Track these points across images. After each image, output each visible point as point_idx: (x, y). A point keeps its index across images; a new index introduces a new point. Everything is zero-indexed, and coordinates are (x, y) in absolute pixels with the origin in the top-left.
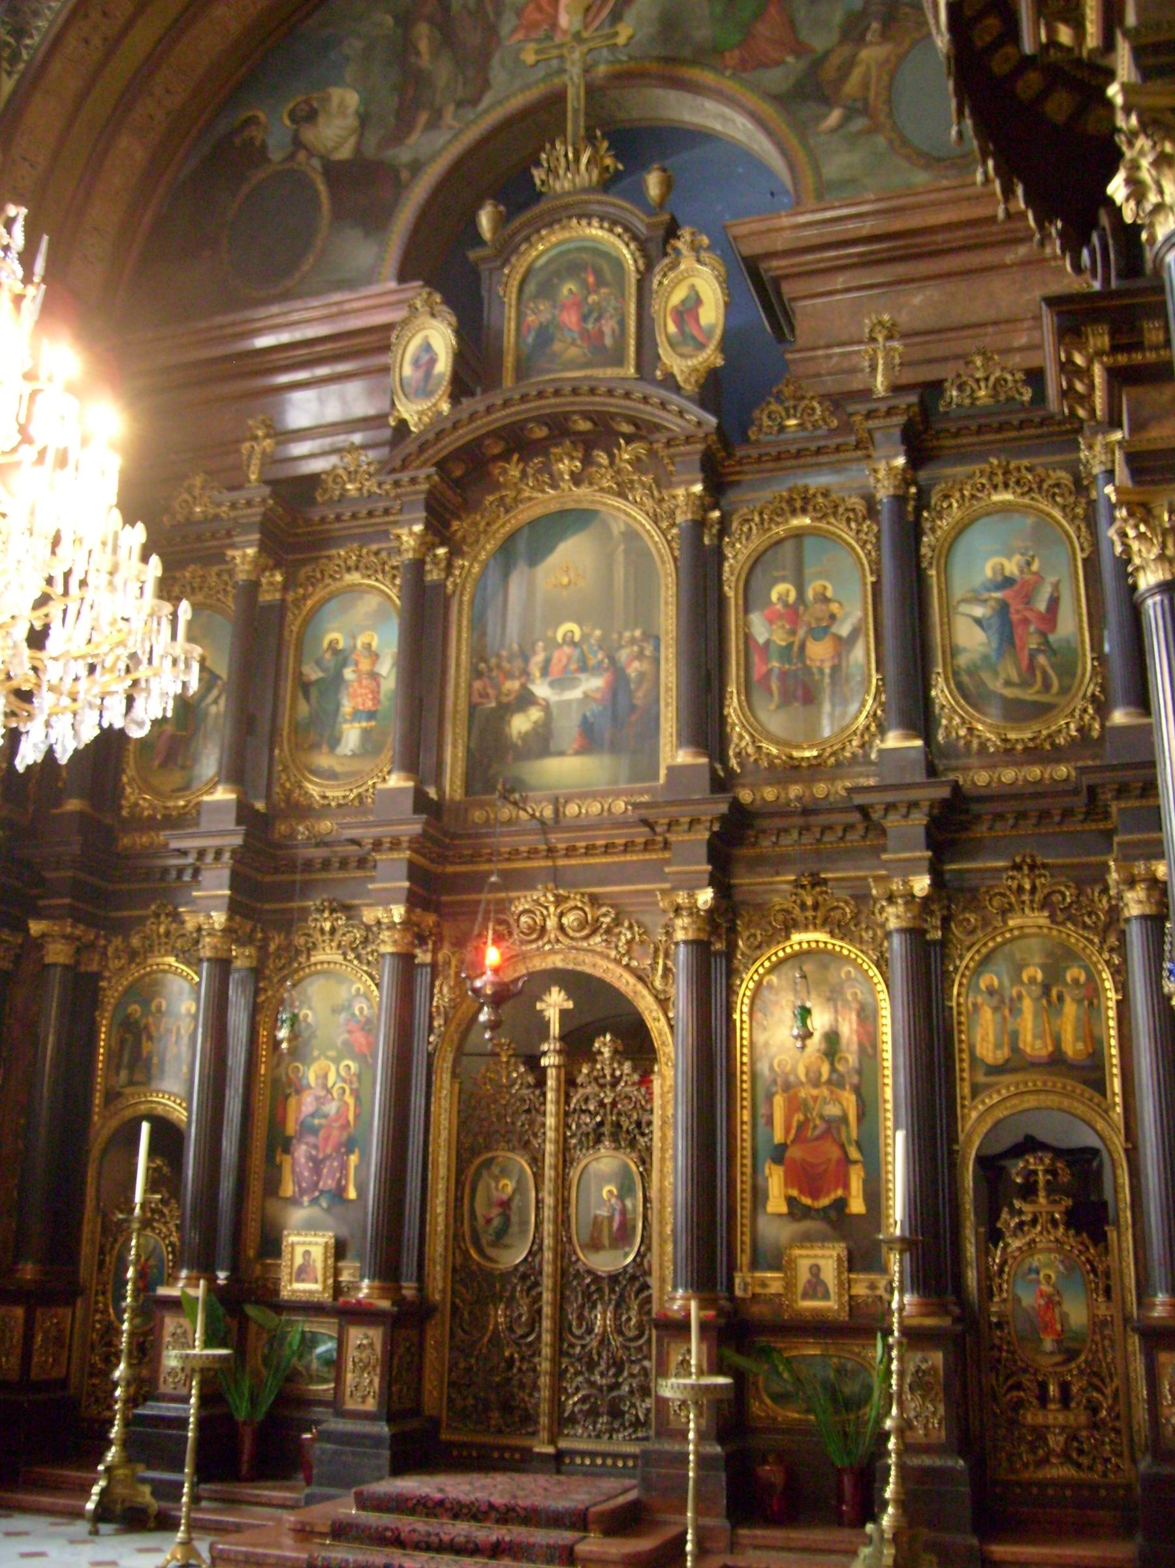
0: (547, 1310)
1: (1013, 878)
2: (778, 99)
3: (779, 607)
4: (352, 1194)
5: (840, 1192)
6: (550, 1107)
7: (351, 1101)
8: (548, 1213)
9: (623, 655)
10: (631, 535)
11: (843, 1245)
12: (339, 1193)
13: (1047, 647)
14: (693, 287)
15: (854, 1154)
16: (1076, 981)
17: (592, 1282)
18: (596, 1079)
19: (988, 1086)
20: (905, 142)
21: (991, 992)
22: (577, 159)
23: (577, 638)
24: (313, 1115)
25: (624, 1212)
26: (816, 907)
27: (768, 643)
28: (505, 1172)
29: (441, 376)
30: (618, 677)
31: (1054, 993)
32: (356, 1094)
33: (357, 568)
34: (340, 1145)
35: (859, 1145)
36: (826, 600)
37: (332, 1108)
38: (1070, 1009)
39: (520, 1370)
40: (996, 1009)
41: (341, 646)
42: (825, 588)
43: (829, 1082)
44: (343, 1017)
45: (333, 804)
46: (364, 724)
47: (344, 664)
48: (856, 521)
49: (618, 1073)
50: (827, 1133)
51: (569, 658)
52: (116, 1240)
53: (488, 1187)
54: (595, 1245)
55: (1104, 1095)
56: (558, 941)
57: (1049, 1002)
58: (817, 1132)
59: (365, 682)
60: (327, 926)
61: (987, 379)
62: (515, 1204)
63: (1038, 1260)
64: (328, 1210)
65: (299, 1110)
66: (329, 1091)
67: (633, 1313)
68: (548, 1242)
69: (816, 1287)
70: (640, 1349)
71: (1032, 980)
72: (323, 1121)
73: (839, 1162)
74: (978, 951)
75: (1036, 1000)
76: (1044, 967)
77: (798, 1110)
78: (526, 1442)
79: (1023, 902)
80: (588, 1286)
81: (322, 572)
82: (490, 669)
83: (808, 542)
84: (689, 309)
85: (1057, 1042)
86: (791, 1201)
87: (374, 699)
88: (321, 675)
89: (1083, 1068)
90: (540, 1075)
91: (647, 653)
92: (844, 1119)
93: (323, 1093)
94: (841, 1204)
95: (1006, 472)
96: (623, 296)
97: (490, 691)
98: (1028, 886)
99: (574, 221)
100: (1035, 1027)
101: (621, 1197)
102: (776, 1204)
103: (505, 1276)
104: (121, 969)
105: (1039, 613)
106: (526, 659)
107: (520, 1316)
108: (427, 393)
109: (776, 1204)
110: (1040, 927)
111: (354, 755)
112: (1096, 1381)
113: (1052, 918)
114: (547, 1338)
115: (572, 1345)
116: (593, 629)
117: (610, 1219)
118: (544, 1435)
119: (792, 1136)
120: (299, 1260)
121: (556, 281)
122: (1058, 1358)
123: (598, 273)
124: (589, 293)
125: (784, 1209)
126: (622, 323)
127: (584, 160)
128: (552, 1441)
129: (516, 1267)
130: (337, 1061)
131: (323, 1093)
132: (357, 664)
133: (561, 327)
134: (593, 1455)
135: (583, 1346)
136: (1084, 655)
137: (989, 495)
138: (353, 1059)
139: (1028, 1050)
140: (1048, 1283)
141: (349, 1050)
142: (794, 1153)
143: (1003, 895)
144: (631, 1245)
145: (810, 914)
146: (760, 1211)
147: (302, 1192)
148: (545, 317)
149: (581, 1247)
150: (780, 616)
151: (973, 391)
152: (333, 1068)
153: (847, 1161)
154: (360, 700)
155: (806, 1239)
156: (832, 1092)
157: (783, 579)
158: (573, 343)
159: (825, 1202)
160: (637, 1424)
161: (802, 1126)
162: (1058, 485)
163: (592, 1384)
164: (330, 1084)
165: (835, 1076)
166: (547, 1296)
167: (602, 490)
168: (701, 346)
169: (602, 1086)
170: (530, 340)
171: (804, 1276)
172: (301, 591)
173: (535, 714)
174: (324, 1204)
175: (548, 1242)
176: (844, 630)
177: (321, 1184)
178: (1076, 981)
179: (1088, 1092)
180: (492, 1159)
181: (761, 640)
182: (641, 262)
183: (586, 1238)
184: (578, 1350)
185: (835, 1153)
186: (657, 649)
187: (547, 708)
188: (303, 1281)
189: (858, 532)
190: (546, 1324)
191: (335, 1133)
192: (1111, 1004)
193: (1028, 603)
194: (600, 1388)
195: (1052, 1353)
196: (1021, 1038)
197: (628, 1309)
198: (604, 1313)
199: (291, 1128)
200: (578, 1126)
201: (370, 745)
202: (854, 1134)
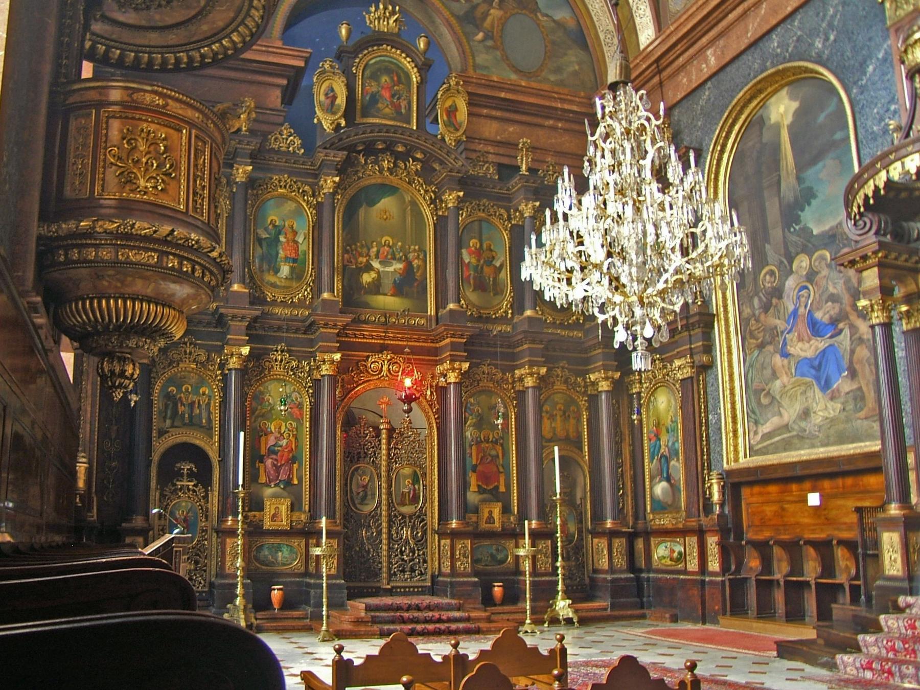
0: (384, 530)
3: (473, 249)
4: (296, 482)
6: (384, 447)
7: (293, 440)
8: (384, 491)
9: (411, 256)
10: (414, 204)
12: (288, 483)
14: (454, 101)
15: (501, 470)
16: (574, 411)
17: (402, 519)
19: (546, 447)
21: (547, 412)
23: (391, 244)
24: (274, 446)
25: (414, 490)
26: (488, 373)
27: (469, 262)
28: (364, 473)
29: (339, 106)
30: (409, 264)
31: (567, 414)
35: (503, 468)
36: (491, 250)
39: (373, 556)
40: (548, 419)
41: (277, 224)
43: (492, 441)
45: (279, 300)
47: (279, 233)
50: (492, 460)
51: (388, 253)
52: (168, 504)
54: (403, 504)
56: (387, 376)
58: (488, 460)
60: (279, 358)
61: (553, 175)
62: (369, 487)
64: (284, 489)
65: (266, 443)
66: (282, 435)
67: (419, 531)
68: (384, 502)
69: (490, 519)
70: (422, 544)
72: (279, 448)
75: (561, 416)
78: (378, 585)
80: (400, 520)
81: (267, 184)
82: (352, 251)
83: (484, 225)
84: (452, 112)
85: (567, 431)
86: (479, 486)
87: (296, 253)
91: (421, 257)
92: (498, 456)
94: (497, 488)
96: (410, 91)
97: (353, 261)
101: (413, 484)
102: (473, 488)
103: (366, 516)
104: (164, 368)
106: (369, 250)
108: (334, 113)
109: (473, 488)
113: (567, 387)
114: (385, 541)
115: (393, 545)
116: (398, 242)
117: (409, 493)
118: (385, 581)
120: (273, 512)
121: (379, 73)
123: (399, 77)
124: (394, 86)
125: (477, 490)
126: (410, 103)
128: (388, 584)
131: (279, 435)
132: (286, 234)
133: (381, 96)
134: (405, 587)
141: (291, 416)
142: (479, 468)
144: (418, 503)
145: (486, 376)
148: (374, 89)
150: (474, 253)
152: (284, 424)
155: (484, 501)
157: (475, 238)
158: (387, 106)
159: (491, 487)
160: (421, 574)
163: (403, 560)
166: (384, 525)
167: (401, 179)
168: (457, 130)
170: (368, 98)
171: (486, 515)
172: (255, 192)
173: (373, 275)
174: (282, 486)
175: (384, 502)
176: (498, 264)
178: (574, 411)
179: (577, 451)
180: (359, 467)
181: (467, 261)
182: (419, 78)
183: (399, 501)
184: (396, 546)
186: (425, 256)
187: (378, 272)
188: (275, 521)
190: (384, 536)
191: (286, 454)
194: (406, 561)
198: (407, 531)
199: (263, 451)
200: (394, 455)
201: (297, 275)
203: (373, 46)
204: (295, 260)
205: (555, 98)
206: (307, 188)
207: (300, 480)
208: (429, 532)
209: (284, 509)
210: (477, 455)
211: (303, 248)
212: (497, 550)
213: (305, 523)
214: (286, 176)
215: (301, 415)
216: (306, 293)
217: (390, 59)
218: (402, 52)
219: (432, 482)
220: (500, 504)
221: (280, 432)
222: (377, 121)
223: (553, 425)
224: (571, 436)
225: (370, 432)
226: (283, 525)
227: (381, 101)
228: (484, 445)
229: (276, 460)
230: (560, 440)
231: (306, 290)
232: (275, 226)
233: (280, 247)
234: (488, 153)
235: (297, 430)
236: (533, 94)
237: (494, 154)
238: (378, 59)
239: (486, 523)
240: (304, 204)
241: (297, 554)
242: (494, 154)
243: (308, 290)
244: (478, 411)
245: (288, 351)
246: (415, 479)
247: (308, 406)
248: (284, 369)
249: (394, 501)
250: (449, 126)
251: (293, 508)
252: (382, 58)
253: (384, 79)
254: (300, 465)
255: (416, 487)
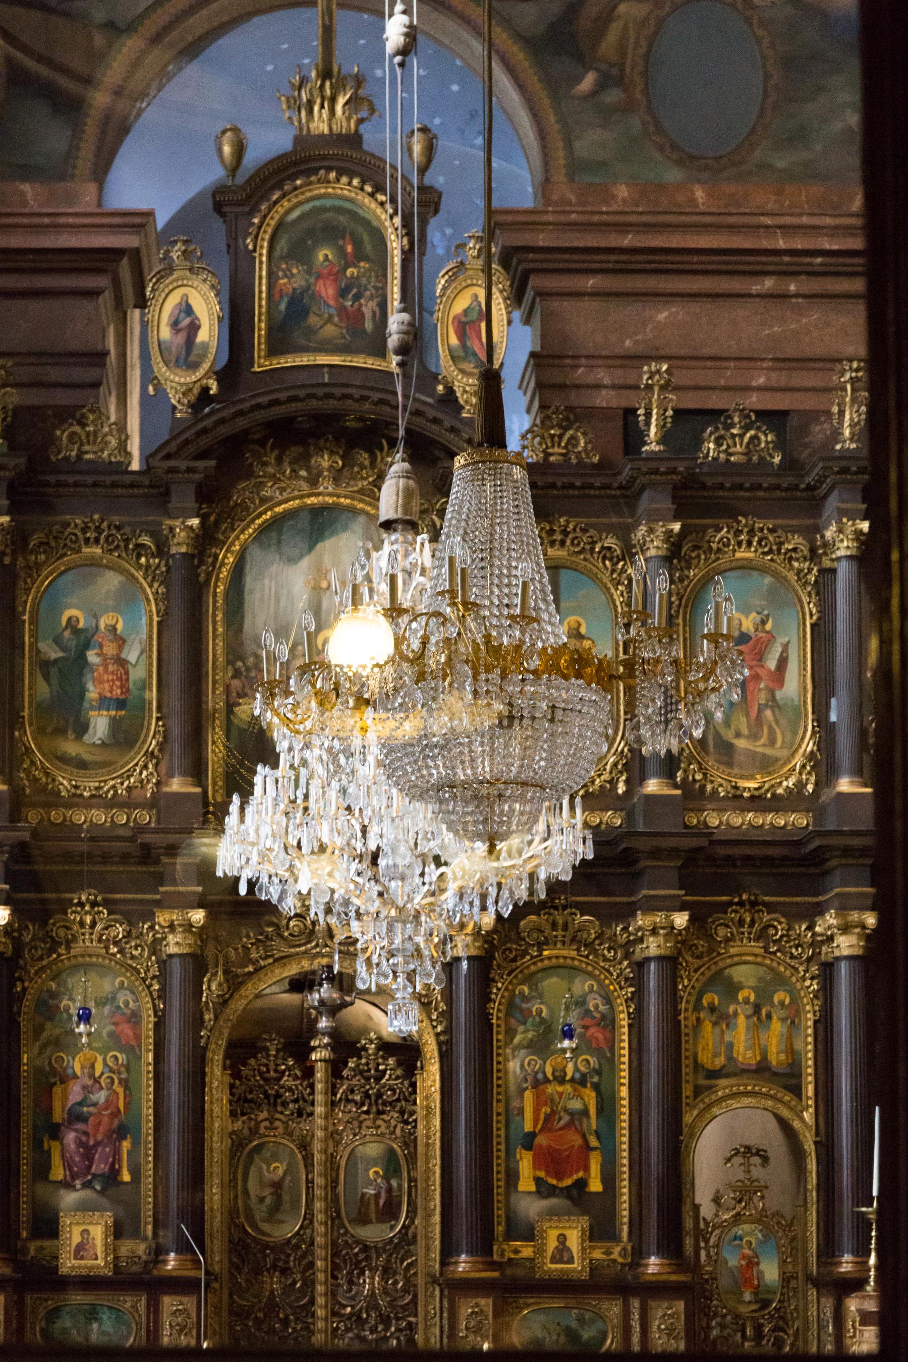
1: (736, 911)
2: (534, 45)
4: (126, 1177)
5: (581, 1174)
6: (319, 1098)
7: (120, 1090)
11: (586, 1218)
13: (773, 703)
15: (594, 1142)
16: (782, 1003)
17: (361, 1251)
18: (361, 1072)
20: (660, 129)
22: (333, 100)
24: (80, 1104)
25: (390, 1190)
28: (275, 1157)
31: (764, 1012)
32: (125, 1083)
33: (97, 541)
34: (113, 1132)
35: (598, 1137)
37: (101, 1097)
38: (777, 1027)
40: (715, 1024)
41: (81, 625)
42: (580, 625)
43: (572, 1080)
44: (107, 1009)
46: (113, 713)
47: (87, 645)
48: (611, 560)
49: (381, 1067)
50: (570, 1124)
53: (260, 1169)
54: (363, 1220)
55: (801, 1099)
57: (759, 1019)
58: (562, 1123)
59: (111, 668)
61: (742, 436)
63: (743, 1229)
64: (102, 1192)
66: (97, 1081)
70: (404, 1308)
71: (747, 1001)
72: (92, 1109)
73: (580, 1147)
74: (702, 974)
75: (748, 1017)
76: (755, 989)
77: (545, 1104)
79: (743, 933)
82: (248, 669)
86: (538, 1181)
87: (121, 687)
88: (60, 654)
89: (784, 1075)
90: (309, 1072)
92: (585, 1112)
93: (90, 1083)
94: (582, 1184)
95: (751, 532)
96: (385, 276)
98: (748, 919)
99: (333, 175)
100: (747, 1040)
101: (386, 1178)
105: (770, 670)
107: (295, 1283)
109: (526, 1184)
110: (756, 955)
111: (103, 744)
112: (781, 1323)
113: (766, 949)
117: (377, 1196)
119: (539, 1126)
122: (754, 1307)
125: (533, 1189)
127: (341, 101)
129: (289, 1241)
130: (104, 1051)
131: (90, 1083)
132: (101, 646)
135: (353, 1307)
136: (806, 716)
137: (734, 551)
138: (121, 1052)
139: (740, 1059)
140: (749, 1248)
141: (116, 1040)
142: (541, 1140)
143: (727, 926)
144: (397, 1218)
146: (512, 1189)
147: (74, 1177)
148: (298, 282)
149: (350, 1222)
151: (729, 447)
152: (100, 1059)
153: (588, 1148)
154: (107, 686)
155: (552, 1213)
156: (575, 1090)
158: (330, 319)
159: (568, 1182)
161: (548, 1118)
162: (795, 550)
164: (97, 1074)
165: (577, 1075)
169: (368, 1079)
170: (283, 307)
174: (98, 1187)
177: (93, 1170)
178: (782, 1003)
180: (264, 1143)
184: (349, 1309)
185: (578, 1141)
189: (613, 571)
191: (105, 1120)
192: (810, 1023)
193: (760, 660)
195: (750, 1302)
196: (735, 1048)
197: (395, 1273)
198: (372, 1278)
199: (58, 1116)
202: (594, 1127)
203: (293, 177)
204: (121, 704)
205: (767, 227)
206: (145, 540)
207: (136, 1173)
208: (421, 1280)
209: (97, 1233)
210: (536, 1112)
211: (137, 674)
212: (581, 1320)
213: (146, 1262)
214: (96, 517)
215: (138, 1037)
216: (145, 773)
217: (337, 203)
218: (363, 182)
219: (428, 1171)
220: (584, 1221)
221: (92, 1075)
222: (304, 360)
223: (727, 1038)
224: (774, 1062)
225: (289, 1069)
226: (98, 1267)
227: (314, 308)
228: (551, 1089)
229: (86, 1133)
230: (744, 1071)
231: (145, 767)
232: (76, 631)
233: (89, 676)
234: (598, 386)
235: (128, 1070)
236: (705, 226)
237: (614, 387)
238: (307, 207)
239: (552, 1262)
240: (139, 575)
241: (129, 1326)
242: (614, 387)
243: (150, 766)
244: (539, 1012)
245: (106, 903)
246: (391, 1164)
247: (152, 1019)
248: (100, 940)
249: (343, 1214)
250: (465, 359)
251: (118, 1231)
252: (317, 203)
253: (324, 254)
254: (136, 1143)
255: (394, 1183)
